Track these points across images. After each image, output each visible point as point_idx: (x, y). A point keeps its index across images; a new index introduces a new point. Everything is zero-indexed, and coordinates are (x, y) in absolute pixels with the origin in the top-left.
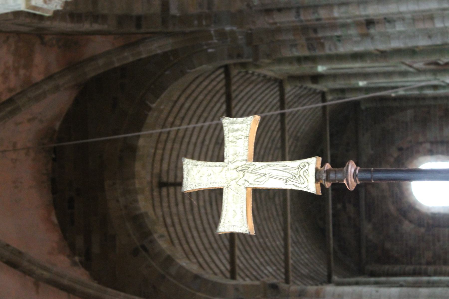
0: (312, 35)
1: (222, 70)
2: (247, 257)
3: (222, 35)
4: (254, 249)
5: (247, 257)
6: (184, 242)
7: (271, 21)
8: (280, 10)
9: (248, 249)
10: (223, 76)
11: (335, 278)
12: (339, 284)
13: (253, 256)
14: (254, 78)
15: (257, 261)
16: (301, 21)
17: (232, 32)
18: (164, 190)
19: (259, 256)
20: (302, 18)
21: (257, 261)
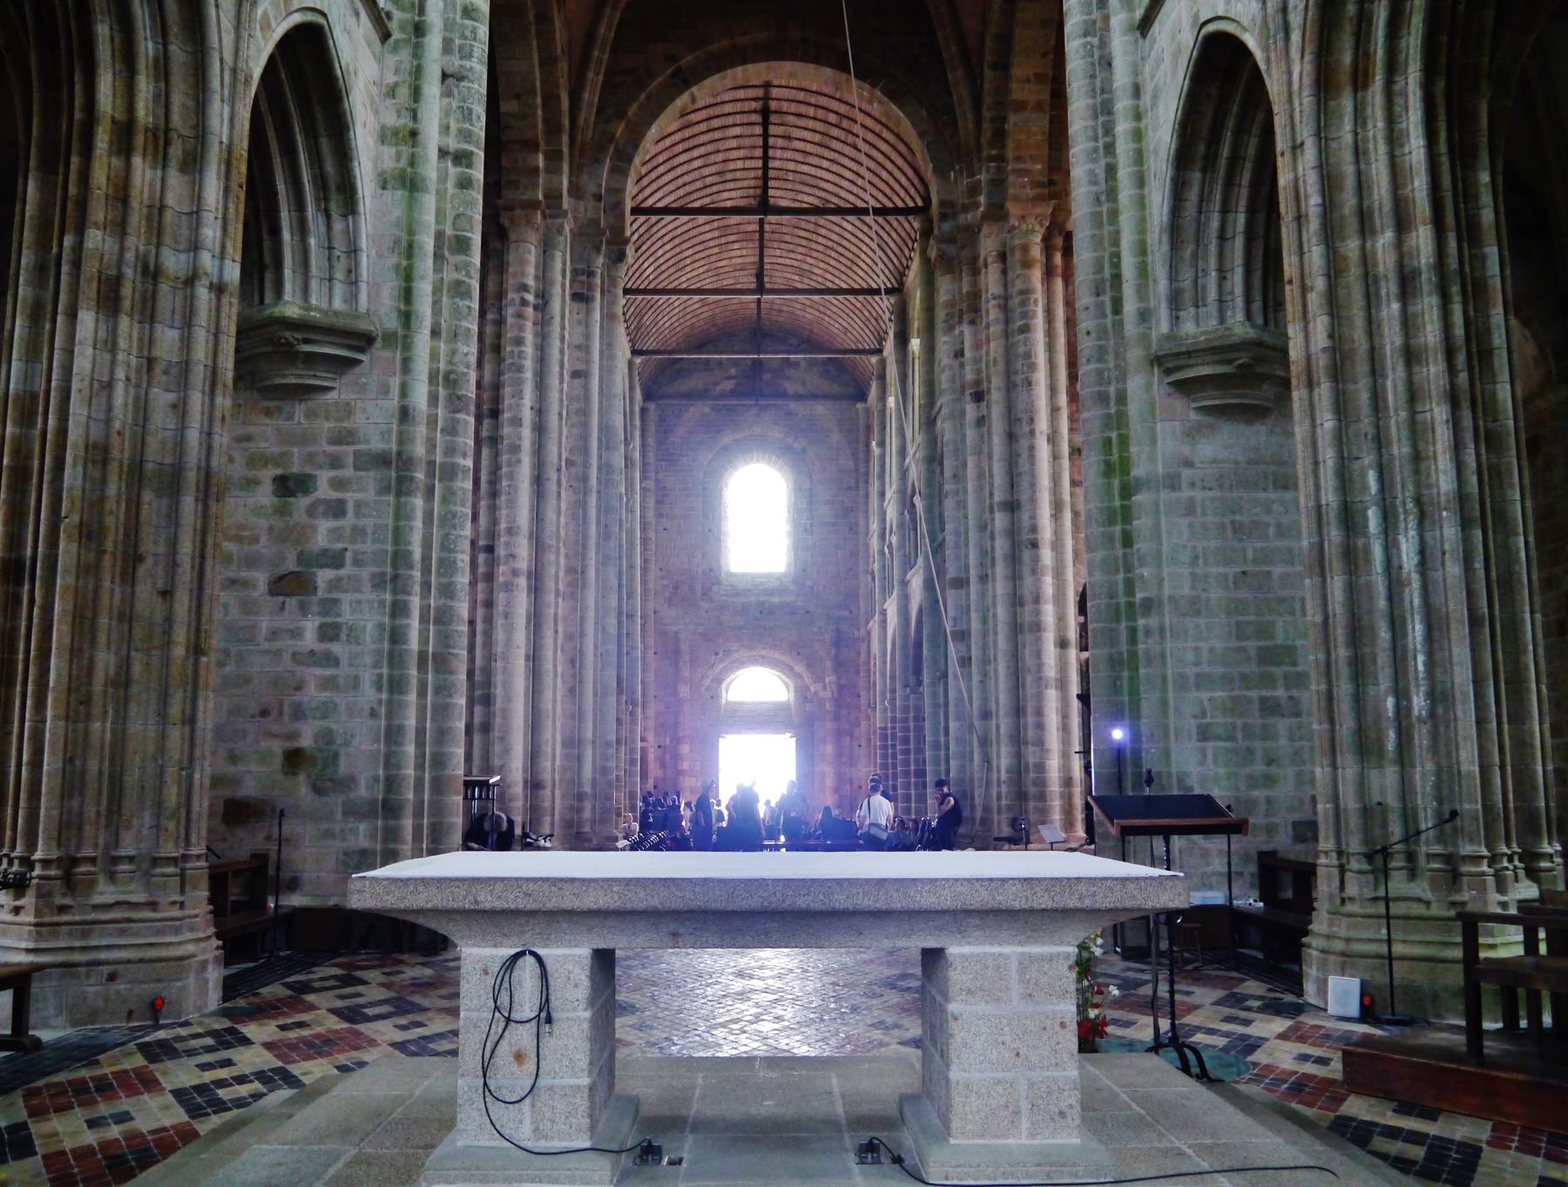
0: (966, 318)
1: (920, 203)
2: (666, 239)
3: (974, 190)
4: (677, 250)
5: (666, 239)
6: (687, 145)
7: (990, 260)
8: (1004, 272)
9: (677, 241)
10: (911, 204)
11: (638, 360)
12: (631, 363)
13: (668, 247)
14: (907, 252)
15: (660, 252)
16: (988, 302)
17: (977, 205)
18: (757, 118)
19: (668, 255)
20: (993, 303)
21: (660, 252)
